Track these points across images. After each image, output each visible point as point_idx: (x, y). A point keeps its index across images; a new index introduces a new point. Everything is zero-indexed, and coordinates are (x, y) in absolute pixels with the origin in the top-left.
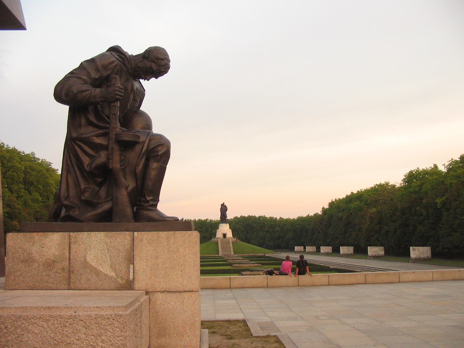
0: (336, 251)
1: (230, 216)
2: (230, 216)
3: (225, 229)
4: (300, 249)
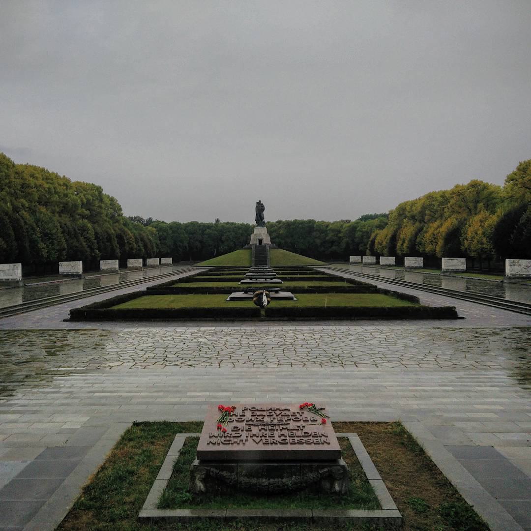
0: (400, 262)
1: (270, 217)
2: (270, 217)
3: (261, 233)
4: (356, 259)
